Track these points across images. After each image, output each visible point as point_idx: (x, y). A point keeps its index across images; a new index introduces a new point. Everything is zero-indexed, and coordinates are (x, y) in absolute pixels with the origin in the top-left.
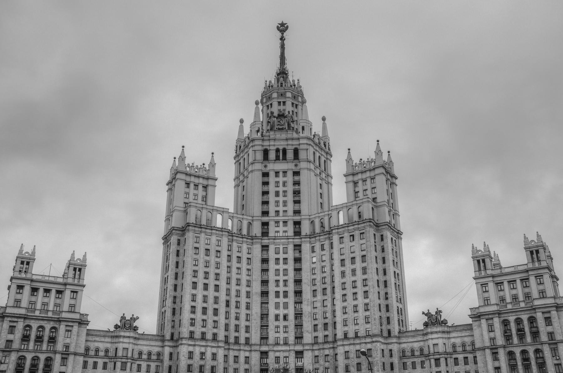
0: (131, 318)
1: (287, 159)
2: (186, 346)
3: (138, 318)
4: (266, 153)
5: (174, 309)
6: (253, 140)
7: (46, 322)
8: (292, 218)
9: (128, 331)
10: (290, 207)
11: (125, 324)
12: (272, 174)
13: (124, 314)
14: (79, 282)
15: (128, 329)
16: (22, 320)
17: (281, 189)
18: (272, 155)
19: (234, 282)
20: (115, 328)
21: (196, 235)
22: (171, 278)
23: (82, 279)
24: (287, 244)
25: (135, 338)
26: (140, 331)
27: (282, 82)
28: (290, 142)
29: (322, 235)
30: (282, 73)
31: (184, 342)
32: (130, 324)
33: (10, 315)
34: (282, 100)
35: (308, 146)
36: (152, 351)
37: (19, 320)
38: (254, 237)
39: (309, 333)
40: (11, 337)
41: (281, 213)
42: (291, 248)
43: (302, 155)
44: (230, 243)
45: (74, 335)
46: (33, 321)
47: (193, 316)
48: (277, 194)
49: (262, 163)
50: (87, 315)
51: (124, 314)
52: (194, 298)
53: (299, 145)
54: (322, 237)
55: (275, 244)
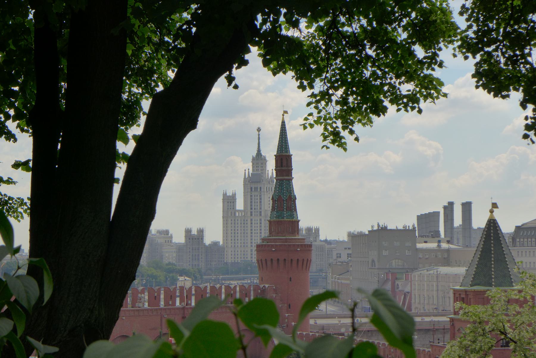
4: (251, 188)
12: (253, 196)
17: (256, 201)
18: (253, 189)
30: (259, 151)
43: (262, 190)
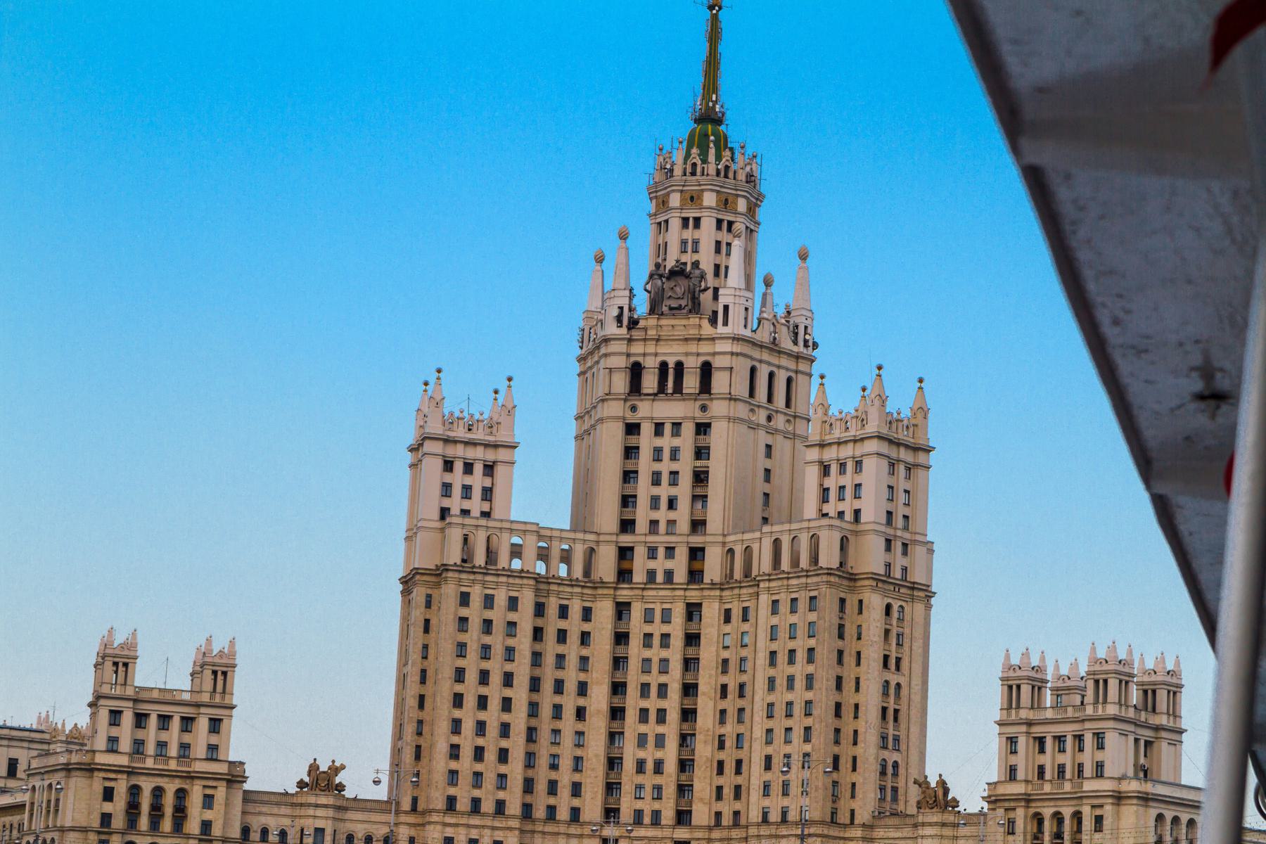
0: (330, 768)
1: (684, 392)
2: (439, 827)
3: (343, 767)
4: (636, 371)
5: (418, 747)
6: (606, 340)
7: (166, 779)
8: (684, 539)
9: (323, 793)
10: (683, 515)
11: (317, 779)
12: (647, 429)
13: (315, 760)
14: (223, 698)
15: (324, 791)
16: (125, 776)
18: (650, 382)
19: (547, 686)
20: (297, 787)
21: (464, 589)
22: (412, 682)
23: (228, 694)
24: (672, 601)
25: (339, 808)
26: (348, 793)
27: (694, 161)
28: (693, 347)
29: (746, 587)
30: (709, 118)
31: (435, 818)
32: (328, 781)
33: (104, 767)
34: (691, 214)
35: (734, 357)
36: (375, 832)
37: (119, 776)
38: (598, 583)
39: (704, 803)
40: (108, 807)
41: (662, 527)
42: (679, 612)
43: (719, 382)
44: (543, 600)
45: (220, 804)
46: (143, 778)
47: (454, 765)
48: (656, 479)
49: (625, 400)
50: (242, 763)
51: (315, 760)
52: (456, 726)
53: (714, 354)
54: (744, 591)
55: (644, 600)
